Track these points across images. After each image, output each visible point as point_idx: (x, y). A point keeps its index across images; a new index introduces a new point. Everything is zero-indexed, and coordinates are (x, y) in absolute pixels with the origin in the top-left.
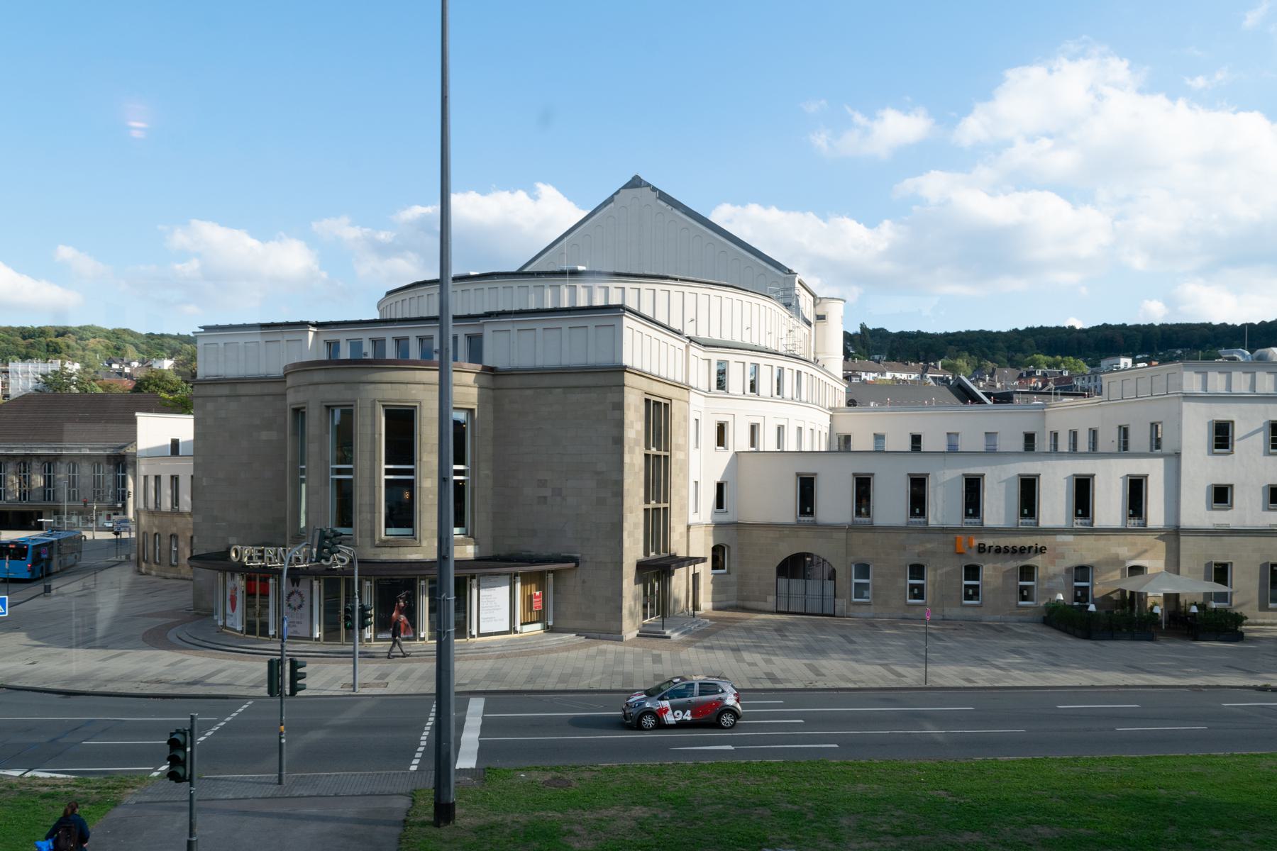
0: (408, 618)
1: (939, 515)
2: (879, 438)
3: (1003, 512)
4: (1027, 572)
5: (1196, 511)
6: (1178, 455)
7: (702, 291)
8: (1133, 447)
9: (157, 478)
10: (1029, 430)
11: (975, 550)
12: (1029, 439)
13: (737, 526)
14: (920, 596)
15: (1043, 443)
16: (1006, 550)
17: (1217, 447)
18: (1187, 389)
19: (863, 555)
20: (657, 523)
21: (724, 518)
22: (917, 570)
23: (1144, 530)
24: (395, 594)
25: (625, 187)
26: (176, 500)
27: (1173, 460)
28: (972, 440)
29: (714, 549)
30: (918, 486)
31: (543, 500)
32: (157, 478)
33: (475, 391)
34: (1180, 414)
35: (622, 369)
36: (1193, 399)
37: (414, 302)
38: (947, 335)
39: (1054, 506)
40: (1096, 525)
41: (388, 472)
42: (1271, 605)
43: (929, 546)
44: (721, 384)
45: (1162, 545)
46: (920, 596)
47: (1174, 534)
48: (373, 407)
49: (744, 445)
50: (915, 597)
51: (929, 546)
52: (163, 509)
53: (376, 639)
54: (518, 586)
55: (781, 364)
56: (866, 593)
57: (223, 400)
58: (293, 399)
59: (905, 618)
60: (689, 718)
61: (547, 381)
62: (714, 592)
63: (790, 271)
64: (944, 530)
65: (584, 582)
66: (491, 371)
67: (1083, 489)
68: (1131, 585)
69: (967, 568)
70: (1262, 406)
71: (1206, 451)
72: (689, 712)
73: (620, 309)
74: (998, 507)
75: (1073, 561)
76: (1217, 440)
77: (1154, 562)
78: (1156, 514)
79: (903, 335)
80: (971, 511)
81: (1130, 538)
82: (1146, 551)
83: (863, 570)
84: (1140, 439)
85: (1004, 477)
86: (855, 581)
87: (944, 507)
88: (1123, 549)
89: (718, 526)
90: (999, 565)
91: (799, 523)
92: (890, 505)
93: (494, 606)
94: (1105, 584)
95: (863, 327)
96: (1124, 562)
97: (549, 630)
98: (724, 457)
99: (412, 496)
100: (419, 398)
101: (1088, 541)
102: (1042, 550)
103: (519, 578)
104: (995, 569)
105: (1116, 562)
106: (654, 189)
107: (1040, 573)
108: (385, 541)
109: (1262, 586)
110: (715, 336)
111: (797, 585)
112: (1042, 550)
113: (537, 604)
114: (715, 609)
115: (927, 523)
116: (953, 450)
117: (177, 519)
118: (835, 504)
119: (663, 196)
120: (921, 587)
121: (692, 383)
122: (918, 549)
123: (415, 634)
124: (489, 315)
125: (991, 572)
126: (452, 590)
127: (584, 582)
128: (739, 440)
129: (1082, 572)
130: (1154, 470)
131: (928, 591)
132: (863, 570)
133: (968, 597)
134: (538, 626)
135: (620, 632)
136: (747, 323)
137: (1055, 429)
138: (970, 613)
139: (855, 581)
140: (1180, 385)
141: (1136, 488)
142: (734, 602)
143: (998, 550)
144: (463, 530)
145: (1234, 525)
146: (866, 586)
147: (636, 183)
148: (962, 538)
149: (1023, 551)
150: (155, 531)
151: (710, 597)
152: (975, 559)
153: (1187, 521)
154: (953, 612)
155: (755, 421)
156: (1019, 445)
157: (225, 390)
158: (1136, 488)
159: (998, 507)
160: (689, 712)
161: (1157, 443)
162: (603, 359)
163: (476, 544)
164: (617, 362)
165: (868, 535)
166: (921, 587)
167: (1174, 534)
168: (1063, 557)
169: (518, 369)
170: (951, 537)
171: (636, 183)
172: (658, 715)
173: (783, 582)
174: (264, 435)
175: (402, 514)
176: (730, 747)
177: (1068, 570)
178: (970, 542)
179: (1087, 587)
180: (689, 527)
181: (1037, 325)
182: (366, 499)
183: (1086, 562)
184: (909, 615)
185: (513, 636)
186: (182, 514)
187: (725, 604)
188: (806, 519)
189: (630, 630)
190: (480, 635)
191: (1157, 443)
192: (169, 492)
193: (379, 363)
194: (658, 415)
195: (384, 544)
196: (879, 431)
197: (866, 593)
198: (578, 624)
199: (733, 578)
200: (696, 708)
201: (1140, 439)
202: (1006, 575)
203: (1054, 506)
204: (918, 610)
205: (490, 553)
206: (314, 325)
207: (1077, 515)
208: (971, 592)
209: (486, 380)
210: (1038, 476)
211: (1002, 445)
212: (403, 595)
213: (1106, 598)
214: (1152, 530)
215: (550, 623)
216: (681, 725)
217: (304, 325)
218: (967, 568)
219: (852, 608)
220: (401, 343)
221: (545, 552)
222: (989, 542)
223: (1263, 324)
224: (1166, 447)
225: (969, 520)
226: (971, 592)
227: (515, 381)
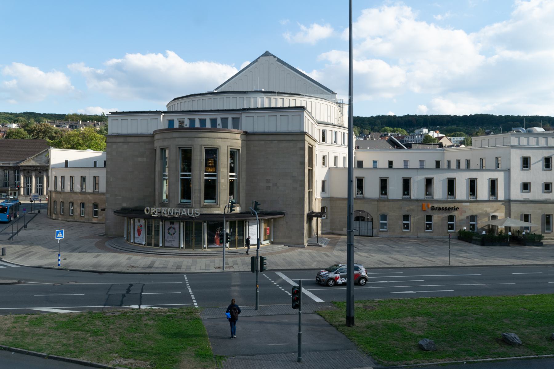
2: (375, 162)
3: (441, 193)
4: (451, 218)
5: (516, 193)
6: (509, 170)
9: (63, 177)
11: (430, 209)
13: (331, 199)
14: (408, 228)
15: (444, 165)
16: (443, 209)
17: (524, 167)
19: (384, 211)
21: (325, 196)
22: (406, 218)
23: (496, 201)
26: (72, 187)
27: (507, 172)
28: (414, 163)
29: (321, 208)
31: (269, 188)
32: (63, 177)
33: (240, 142)
34: (510, 154)
35: (305, 133)
39: (461, 191)
40: (478, 199)
42: (546, 231)
43: (411, 207)
45: (503, 207)
46: (408, 228)
47: (508, 202)
48: (201, 148)
49: (332, 165)
50: (405, 228)
51: (411, 207)
52: (65, 191)
53: (208, 248)
54: (263, 224)
56: (385, 227)
57: (121, 144)
61: (271, 138)
63: (333, 93)
64: (418, 201)
66: (246, 133)
67: (472, 184)
69: (382, 216)
70: (541, 151)
71: (520, 169)
73: (302, 108)
74: (439, 191)
75: (469, 213)
76: (524, 164)
77: (501, 215)
78: (501, 194)
80: (383, 192)
81: (491, 204)
82: (498, 210)
85: (441, 179)
88: (489, 209)
89: (323, 199)
93: (252, 231)
94: (482, 223)
98: (325, 170)
100: (220, 144)
101: (475, 205)
102: (457, 209)
103: (263, 221)
104: (438, 217)
108: (206, 205)
109: (542, 224)
110: (322, 120)
112: (457, 209)
113: (268, 232)
115: (410, 198)
116: (375, 168)
117: (73, 195)
118: (372, 190)
119: (279, 60)
120: (408, 224)
124: (244, 109)
125: (437, 218)
128: (330, 163)
129: (473, 218)
130: (500, 176)
131: (411, 226)
132: (384, 217)
133: (427, 229)
134: (268, 242)
136: (329, 115)
137: (449, 159)
138: (428, 235)
140: (510, 142)
141: (493, 183)
142: (329, 231)
143: (440, 209)
145: (531, 199)
148: (425, 204)
149: (449, 209)
150: (61, 200)
152: (430, 213)
153: (513, 197)
154: (422, 234)
155: (324, 154)
156: (434, 166)
157: (122, 140)
158: (493, 183)
159: (439, 191)
162: (295, 129)
163: (240, 206)
164: (301, 130)
165: (386, 203)
166: (408, 224)
167: (508, 202)
169: (257, 133)
170: (421, 204)
177: (467, 217)
178: (428, 206)
179: (474, 224)
181: (381, 115)
183: (474, 214)
184: (404, 236)
186: (76, 193)
192: (69, 183)
193: (203, 129)
195: (205, 207)
196: (375, 159)
197: (385, 227)
198: (284, 241)
199: (328, 221)
203: (461, 191)
204: (407, 234)
205: (244, 211)
209: (244, 137)
210: (455, 179)
211: (426, 166)
214: (500, 201)
215: (272, 240)
218: (404, 216)
219: (380, 233)
220: (203, 121)
221: (269, 210)
222: (436, 205)
223: (471, 115)
225: (450, 197)
227: (256, 138)
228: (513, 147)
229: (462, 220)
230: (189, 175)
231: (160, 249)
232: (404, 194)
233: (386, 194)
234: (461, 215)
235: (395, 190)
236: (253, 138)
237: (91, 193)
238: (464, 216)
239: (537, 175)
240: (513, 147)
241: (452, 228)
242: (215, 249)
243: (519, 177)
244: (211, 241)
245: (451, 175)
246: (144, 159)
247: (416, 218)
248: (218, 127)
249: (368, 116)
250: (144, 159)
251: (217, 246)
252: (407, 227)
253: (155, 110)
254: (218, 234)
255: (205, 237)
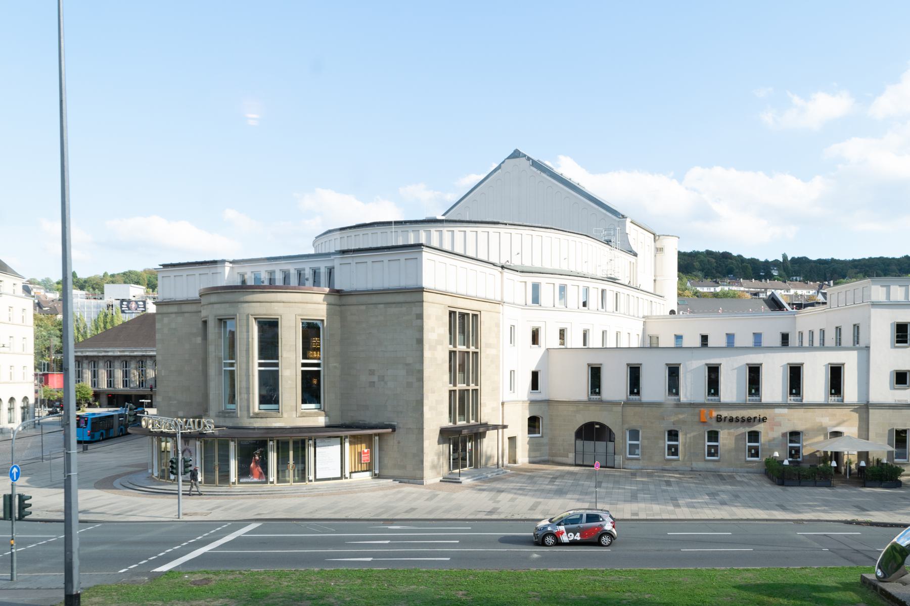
0: (262, 468)
1: (688, 394)
2: (679, 338)
4: (754, 436)
5: (882, 390)
6: (868, 348)
7: (526, 232)
10: (785, 331)
11: (714, 420)
12: (785, 338)
13: (548, 402)
14: (676, 453)
15: (793, 341)
16: (737, 420)
17: (898, 342)
18: (874, 298)
19: (634, 423)
20: (463, 402)
21: (537, 396)
23: (842, 405)
24: (254, 451)
25: (508, 158)
27: (865, 352)
30: (674, 372)
31: (372, 384)
34: (869, 318)
35: (421, 290)
36: (878, 308)
37: (327, 243)
38: (854, 261)
39: (773, 387)
40: (805, 401)
41: (260, 365)
43: (681, 417)
44: (536, 300)
45: (856, 416)
46: (676, 453)
48: (248, 319)
49: (555, 342)
51: (681, 417)
53: (239, 482)
54: (347, 445)
55: (587, 284)
56: (637, 452)
59: (664, 470)
60: (579, 538)
61: (375, 299)
62: (530, 450)
63: (623, 217)
65: (399, 443)
66: (339, 293)
67: (795, 374)
68: (833, 446)
71: (889, 345)
72: (578, 534)
73: (419, 246)
74: (732, 388)
76: (898, 337)
77: (850, 429)
79: (820, 262)
81: (830, 411)
82: (844, 421)
83: (634, 434)
84: (847, 337)
85: (736, 366)
86: (629, 442)
87: (692, 387)
88: (827, 419)
89: (532, 402)
90: (732, 431)
91: (589, 400)
92: (654, 386)
93: (327, 458)
94: (810, 446)
95: (785, 257)
96: (826, 429)
97: (376, 476)
98: (537, 352)
99: (319, 381)
101: (799, 413)
102: (764, 420)
103: (347, 440)
104: (729, 434)
105: (822, 430)
106: (529, 159)
107: (763, 439)
108: (257, 414)
111: (589, 445)
112: (764, 420)
113: (366, 458)
114: (530, 462)
118: (615, 386)
120: (676, 447)
121: (505, 300)
122: (673, 419)
123: (267, 478)
125: (727, 437)
126: (296, 446)
127: (399, 443)
128: (549, 339)
129: (795, 435)
130: (849, 360)
132: (634, 434)
133: (710, 454)
134: (368, 474)
135: (422, 478)
138: (711, 466)
139: (629, 442)
141: (836, 373)
142: (546, 458)
143: (731, 420)
144: (317, 406)
146: (637, 446)
147: (516, 154)
148: (705, 411)
151: (527, 454)
152: (715, 426)
154: (699, 465)
156: (778, 341)
158: (836, 373)
159: (732, 388)
160: (578, 534)
161: (856, 340)
162: (410, 283)
163: (326, 415)
167: (864, 408)
168: (779, 424)
169: (356, 291)
170: (697, 410)
171: (516, 154)
172: (556, 536)
173: (580, 443)
175: (270, 395)
176: (370, 559)
177: (784, 435)
180: (503, 404)
182: (244, 384)
183: (798, 428)
184: (667, 467)
185: (344, 480)
187: (538, 459)
188: (595, 397)
189: (431, 477)
190: (316, 480)
191: (856, 340)
194: (463, 324)
195: (257, 416)
196: (678, 333)
197: (637, 452)
198: (396, 472)
199: (545, 440)
200: (583, 532)
201: (847, 337)
202: (738, 438)
203: (773, 387)
204: (674, 464)
205: (339, 421)
206: (231, 262)
207: (791, 393)
208: (713, 451)
209: (332, 299)
212: (258, 451)
213: (813, 455)
215: (377, 472)
216: (573, 543)
217: (223, 261)
219: (627, 462)
221: (374, 421)
222: (725, 413)
224: (862, 343)
226: (713, 451)
228: (875, 305)
229: (774, 439)
231: (171, 484)
232: (709, 393)
233: (638, 393)
234: (772, 429)
235: (692, 387)
238: (777, 433)
239: (889, 358)
240: (875, 305)
241: (756, 455)
242: (251, 485)
244: (244, 472)
245: (754, 358)
247: (688, 436)
249: (898, 256)
251: (256, 480)
252: (674, 451)
253: (212, 259)
254: (256, 462)
255: (233, 465)
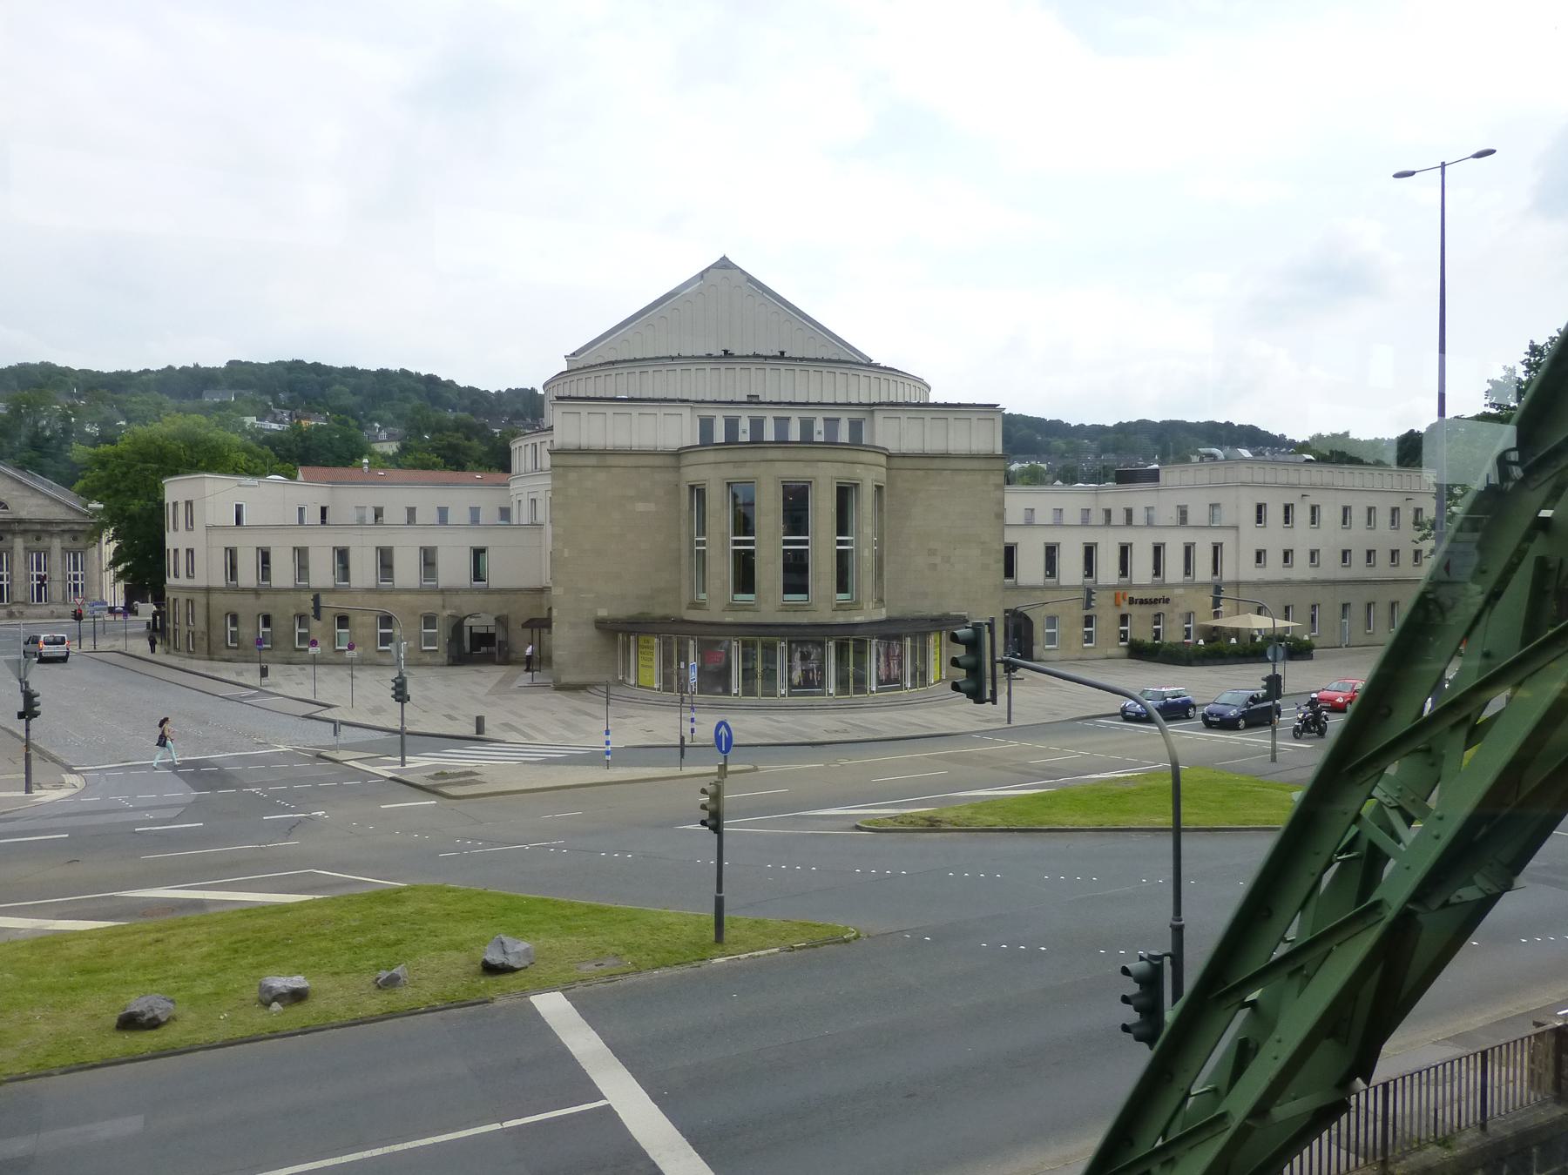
5: (1250, 572)
8: (1191, 520)
46: (1089, 640)
58: (692, 475)
64: (1108, 587)
74: (1142, 569)
75: (1182, 609)
102: (1167, 601)
112: (1167, 601)
120: (1089, 634)
143: (1142, 602)
145: (1267, 578)
152: (1126, 608)
166: (1089, 634)
174: (640, 507)
222: (1136, 595)
230: (751, 543)
236: (896, 463)
237: (369, 590)
243: (1253, 538)
246: (652, 507)
248: (817, 438)
250: (652, 507)
